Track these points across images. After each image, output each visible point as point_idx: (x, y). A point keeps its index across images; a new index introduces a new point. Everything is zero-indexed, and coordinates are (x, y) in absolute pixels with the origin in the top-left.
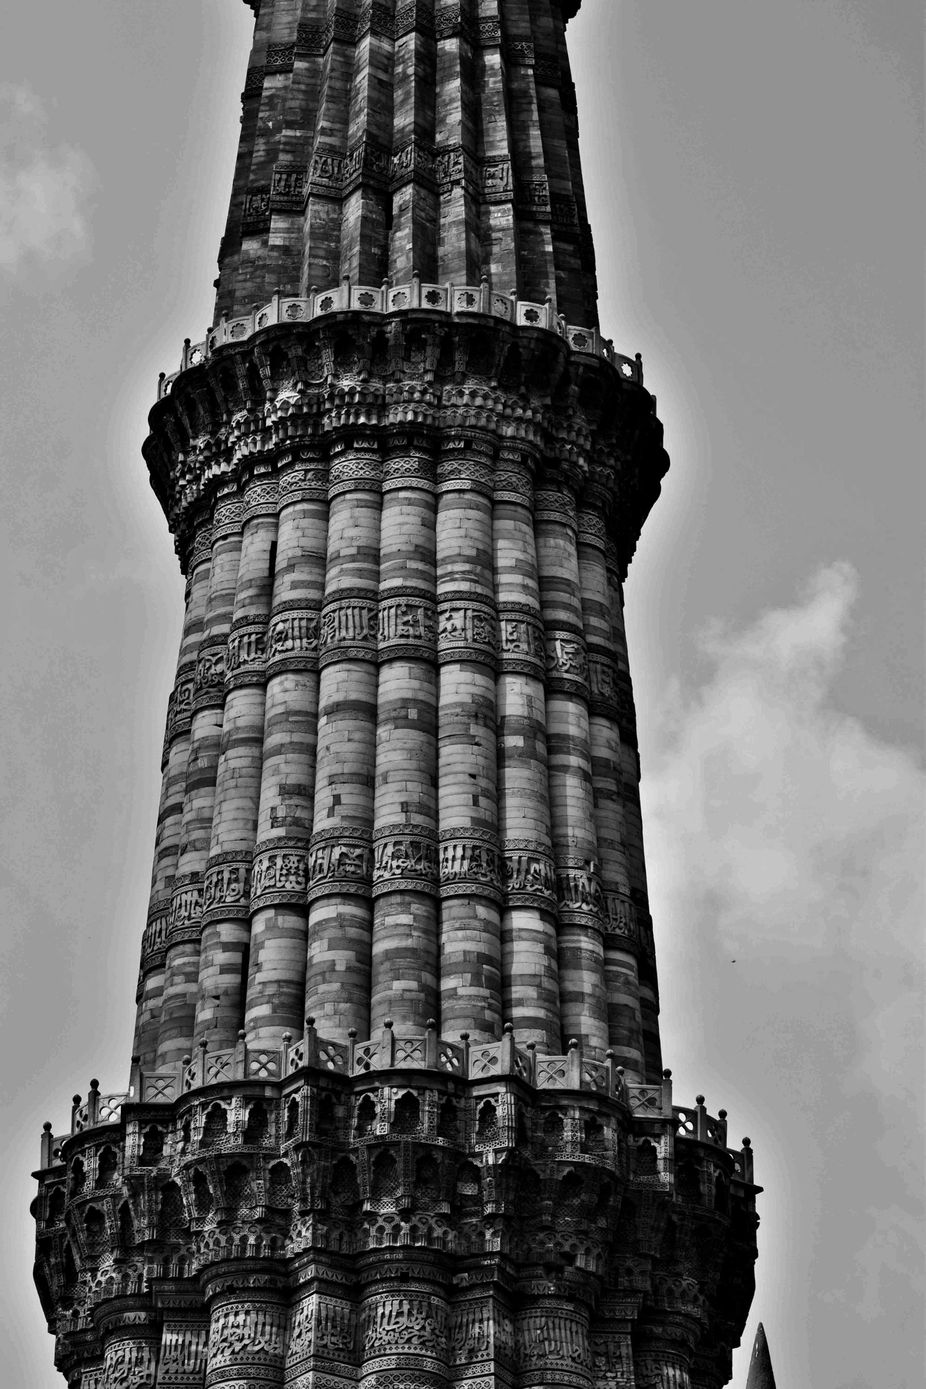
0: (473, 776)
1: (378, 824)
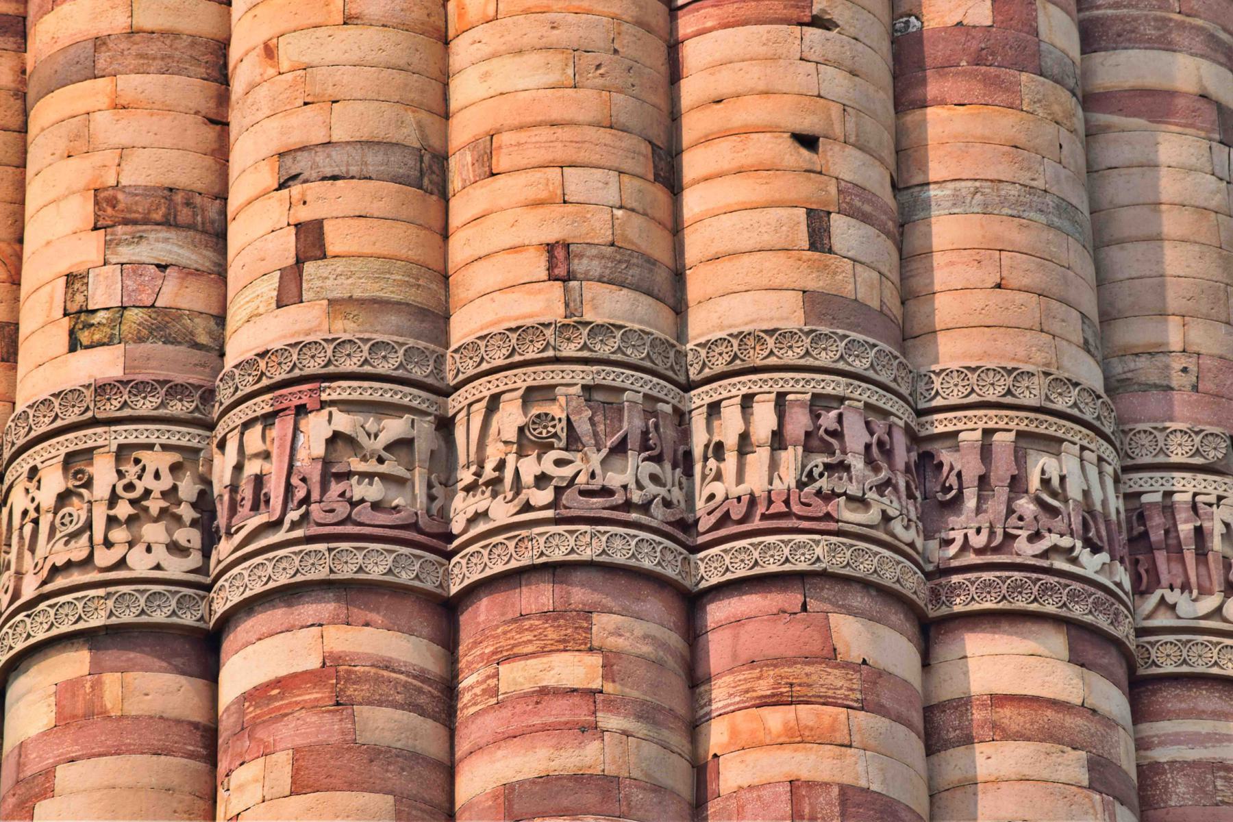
0: (808, 141)
1: (462, 328)
